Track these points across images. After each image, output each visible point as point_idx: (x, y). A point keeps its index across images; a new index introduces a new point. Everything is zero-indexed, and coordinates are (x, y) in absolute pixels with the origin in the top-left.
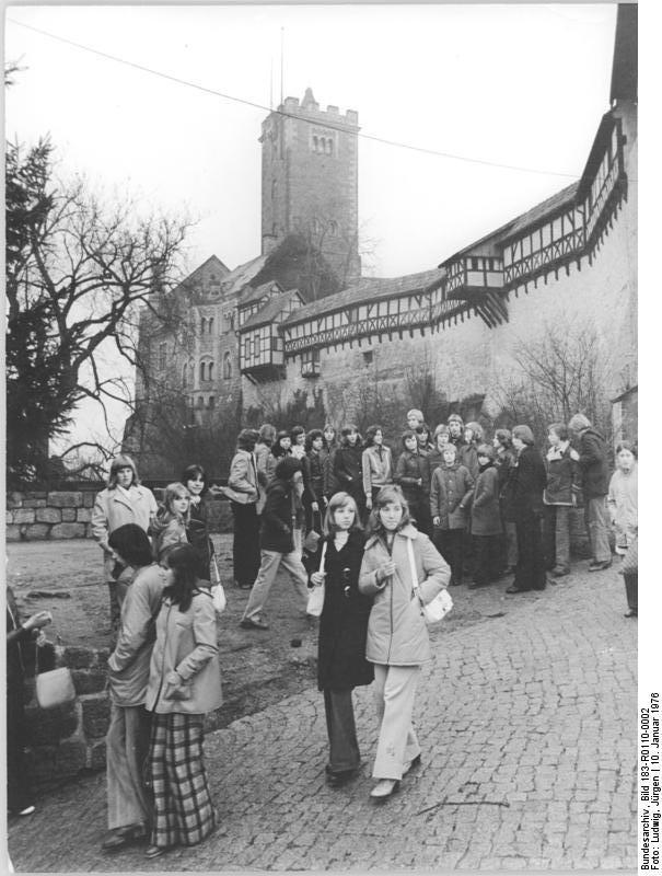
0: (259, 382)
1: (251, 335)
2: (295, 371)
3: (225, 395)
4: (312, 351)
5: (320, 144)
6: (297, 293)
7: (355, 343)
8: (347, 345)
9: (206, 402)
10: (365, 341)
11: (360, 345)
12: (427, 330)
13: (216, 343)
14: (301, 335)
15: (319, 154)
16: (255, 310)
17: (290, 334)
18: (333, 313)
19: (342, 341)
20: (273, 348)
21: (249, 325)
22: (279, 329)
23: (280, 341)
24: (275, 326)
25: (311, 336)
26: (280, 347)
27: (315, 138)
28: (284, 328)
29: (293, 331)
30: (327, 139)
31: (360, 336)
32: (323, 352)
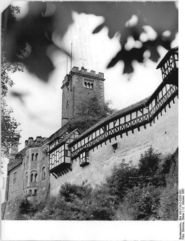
0: (59, 176)
2: (76, 164)
3: (42, 188)
5: (88, 85)
6: (77, 130)
8: (103, 144)
9: (33, 192)
10: (113, 140)
11: (110, 142)
12: (148, 125)
13: (38, 165)
14: (79, 146)
15: (87, 89)
18: (95, 130)
19: (101, 142)
20: (66, 155)
24: (66, 145)
26: (69, 154)
27: (85, 83)
28: (71, 145)
30: (91, 83)
31: (110, 137)
32: (91, 152)
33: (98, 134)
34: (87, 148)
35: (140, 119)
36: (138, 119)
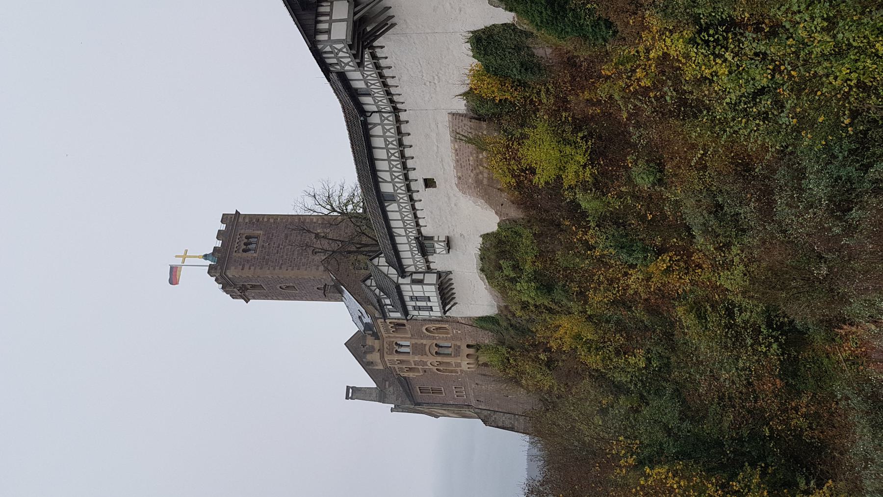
1: (410, 304)
2: (440, 261)
4: (424, 245)
7: (415, 196)
8: (418, 205)
10: (413, 186)
14: (409, 255)
16: (388, 301)
17: (410, 266)
20: (420, 282)
21: (400, 306)
22: (403, 277)
23: (415, 276)
25: (409, 243)
26: (420, 277)
28: (402, 273)
29: (406, 262)
32: (425, 232)
33: (397, 216)
34: (417, 238)
35: (388, 130)
36: (388, 134)
